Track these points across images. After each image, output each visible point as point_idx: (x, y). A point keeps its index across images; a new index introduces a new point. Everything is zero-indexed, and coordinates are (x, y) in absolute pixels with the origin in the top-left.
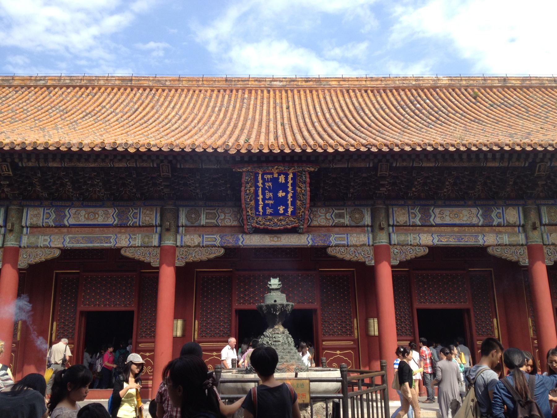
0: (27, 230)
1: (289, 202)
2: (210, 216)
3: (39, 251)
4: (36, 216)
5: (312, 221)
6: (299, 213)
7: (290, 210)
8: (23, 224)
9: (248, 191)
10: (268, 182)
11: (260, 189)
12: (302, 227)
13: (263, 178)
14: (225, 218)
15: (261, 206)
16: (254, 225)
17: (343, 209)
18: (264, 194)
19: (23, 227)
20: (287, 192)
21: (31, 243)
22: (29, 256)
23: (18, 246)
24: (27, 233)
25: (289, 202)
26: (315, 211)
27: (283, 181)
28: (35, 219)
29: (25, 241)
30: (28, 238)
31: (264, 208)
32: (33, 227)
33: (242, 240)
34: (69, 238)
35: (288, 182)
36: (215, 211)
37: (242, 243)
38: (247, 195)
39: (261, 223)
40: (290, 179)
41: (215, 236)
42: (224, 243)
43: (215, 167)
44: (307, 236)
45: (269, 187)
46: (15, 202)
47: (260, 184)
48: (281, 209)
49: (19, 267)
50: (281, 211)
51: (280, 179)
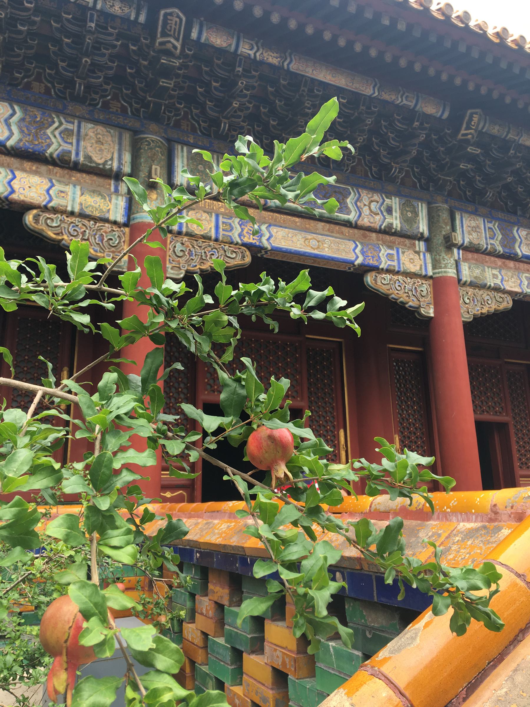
0: (459, 254)
3: (485, 295)
4: (475, 229)
21: (476, 277)
30: (469, 268)
32: (472, 249)
34: (526, 277)
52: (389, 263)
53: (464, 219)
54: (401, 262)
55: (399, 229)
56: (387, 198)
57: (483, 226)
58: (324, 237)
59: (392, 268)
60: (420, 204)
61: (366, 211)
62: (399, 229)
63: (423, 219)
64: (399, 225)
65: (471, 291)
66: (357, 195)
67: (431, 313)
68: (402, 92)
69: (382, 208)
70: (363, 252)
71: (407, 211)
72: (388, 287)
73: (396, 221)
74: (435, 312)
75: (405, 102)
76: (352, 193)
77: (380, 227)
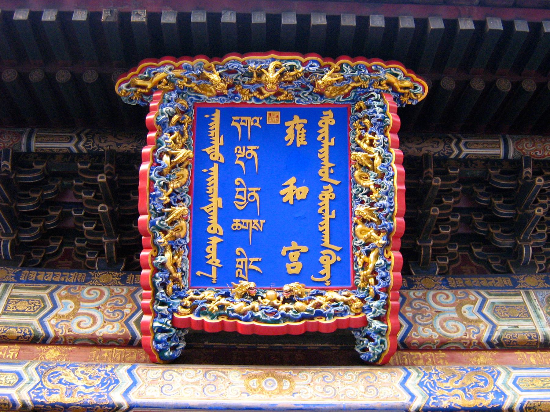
1: (325, 226)
2: (22, 306)
5: (410, 326)
6: (365, 264)
7: (327, 260)
9: (166, 159)
10: (245, 142)
11: (215, 169)
12: (377, 324)
13: (226, 128)
14: (75, 314)
15: (215, 241)
16: (183, 314)
17: (519, 295)
18: (227, 190)
20: (316, 186)
25: (325, 226)
26: (419, 298)
27: (301, 141)
31: (225, 250)
33: (126, 381)
35: (320, 145)
36: (44, 294)
37: (126, 393)
38: (161, 174)
39: (213, 306)
40: (324, 132)
41: (19, 368)
42: (50, 393)
43: (71, 146)
44: (400, 373)
45: (248, 161)
47: (214, 152)
48: (294, 257)
50: (295, 266)
51: (290, 132)
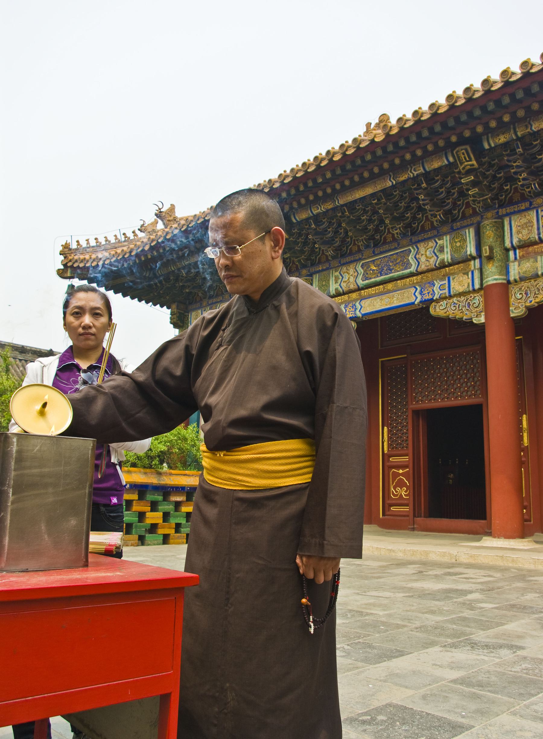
0: (515, 254)
8: (508, 244)
19: (507, 250)
22: (526, 294)
23: (505, 282)
24: (516, 258)
28: (525, 232)
29: (515, 271)
30: (519, 265)
46: (489, 215)
49: (512, 315)
52: (441, 292)
53: (513, 223)
54: (452, 287)
55: (450, 261)
56: (439, 240)
57: (535, 218)
58: (394, 293)
59: (443, 296)
60: (467, 231)
61: (423, 259)
62: (450, 261)
63: (470, 243)
64: (450, 258)
65: (525, 284)
66: (416, 249)
67: (482, 320)
68: (410, 169)
69: (436, 251)
70: (421, 293)
71: (456, 242)
72: (446, 310)
73: (446, 257)
74: (486, 318)
75: (415, 173)
76: (412, 250)
77: (435, 265)
